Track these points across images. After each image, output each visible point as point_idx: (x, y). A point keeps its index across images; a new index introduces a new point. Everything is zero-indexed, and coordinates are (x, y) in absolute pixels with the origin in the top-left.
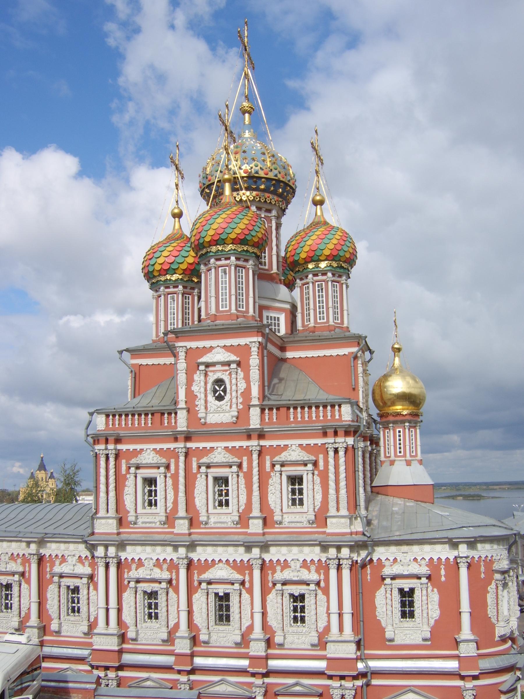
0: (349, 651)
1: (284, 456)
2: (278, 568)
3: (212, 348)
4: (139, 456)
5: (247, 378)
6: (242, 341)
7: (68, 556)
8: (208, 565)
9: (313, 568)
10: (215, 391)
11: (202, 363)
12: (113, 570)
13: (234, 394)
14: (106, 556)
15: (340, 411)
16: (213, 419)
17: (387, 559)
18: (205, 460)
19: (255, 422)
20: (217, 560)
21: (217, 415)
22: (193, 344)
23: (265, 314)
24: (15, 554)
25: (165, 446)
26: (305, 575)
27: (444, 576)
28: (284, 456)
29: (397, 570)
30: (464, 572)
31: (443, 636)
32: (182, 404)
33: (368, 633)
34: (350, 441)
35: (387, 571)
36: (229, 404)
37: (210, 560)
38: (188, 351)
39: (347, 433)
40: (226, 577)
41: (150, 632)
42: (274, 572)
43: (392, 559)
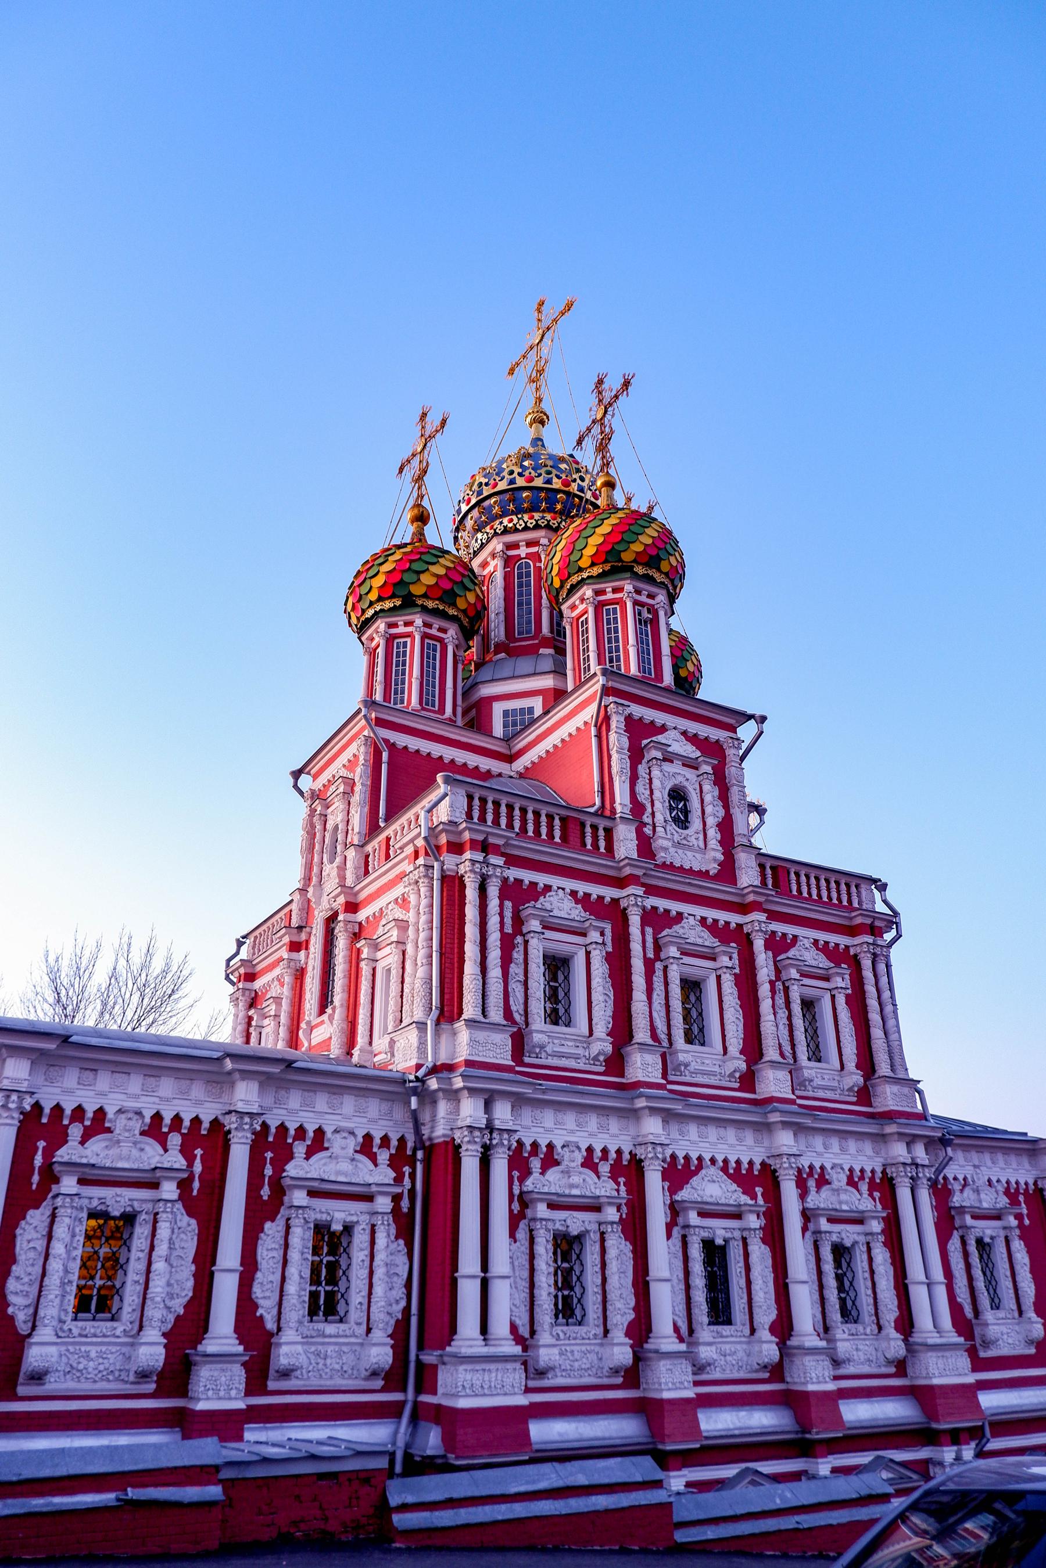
3: (663, 729)
4: (542, 898)
7: (336, 1131)
9: (864, 1187)
12: (500, 1167)
13: (711, 821)
14: (490, 1127)
15: (859, 896)
17: (955, 1179)
20: (707, 1157)
21: (680, 851)
22: (638, 711)
24: (168, 1118)
25: (596, 890)
27: (1028, 1215)
36: (701, 836)
37: (694, 1156)
40: (723, 1201)
41: (575, 1348)
43: (961, 1177)
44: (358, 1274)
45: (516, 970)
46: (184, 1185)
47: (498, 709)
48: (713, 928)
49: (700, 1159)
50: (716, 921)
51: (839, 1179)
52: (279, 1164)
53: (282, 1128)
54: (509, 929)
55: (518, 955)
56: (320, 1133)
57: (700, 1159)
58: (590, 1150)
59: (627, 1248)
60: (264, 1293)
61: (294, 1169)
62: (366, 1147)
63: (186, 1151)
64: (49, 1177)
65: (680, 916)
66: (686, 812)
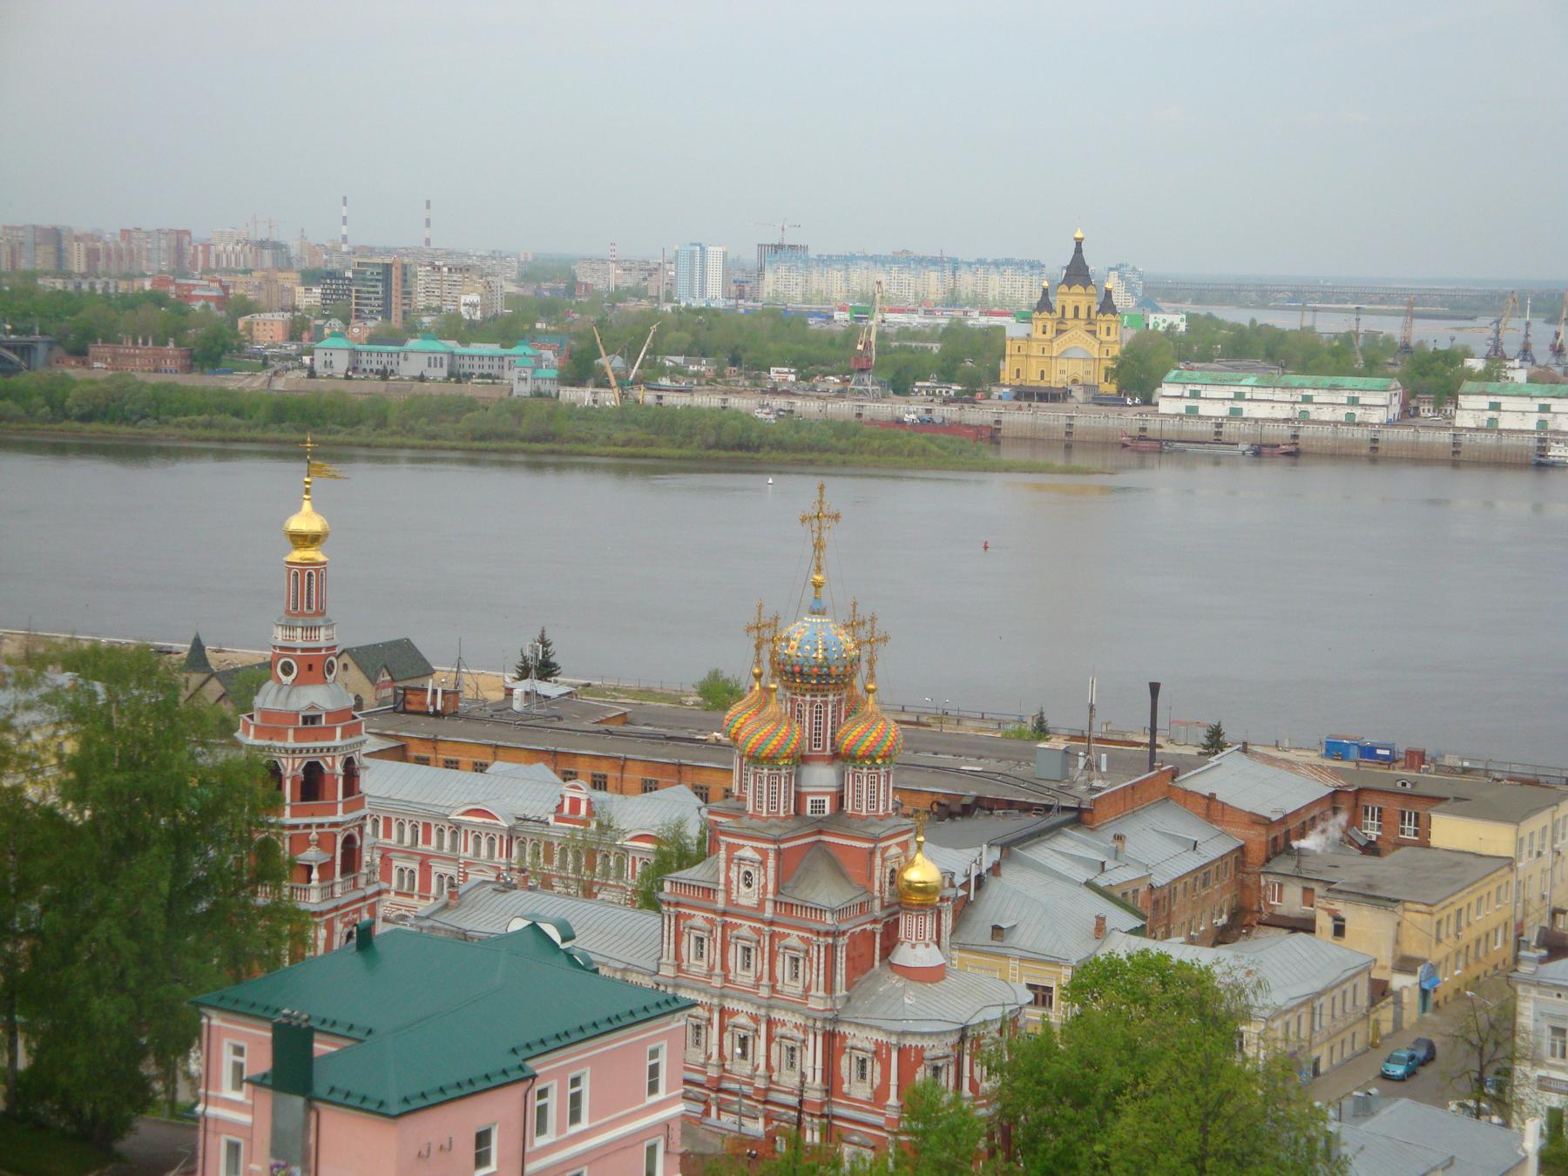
1: (787, 942)
6: (765, 846)
8: (734, 1013)
16: (743, 901)
22: (732, 840)
23: (809, 799)
28: (787, 942)
29: (855, 1042)
30: (894, 1055)
31: (880, 1096)
32: (722, 887)
34: (830, 940)
35: (849, 1042)
38: (728, 845)
39: (827, 934)
51: (790, 1025)
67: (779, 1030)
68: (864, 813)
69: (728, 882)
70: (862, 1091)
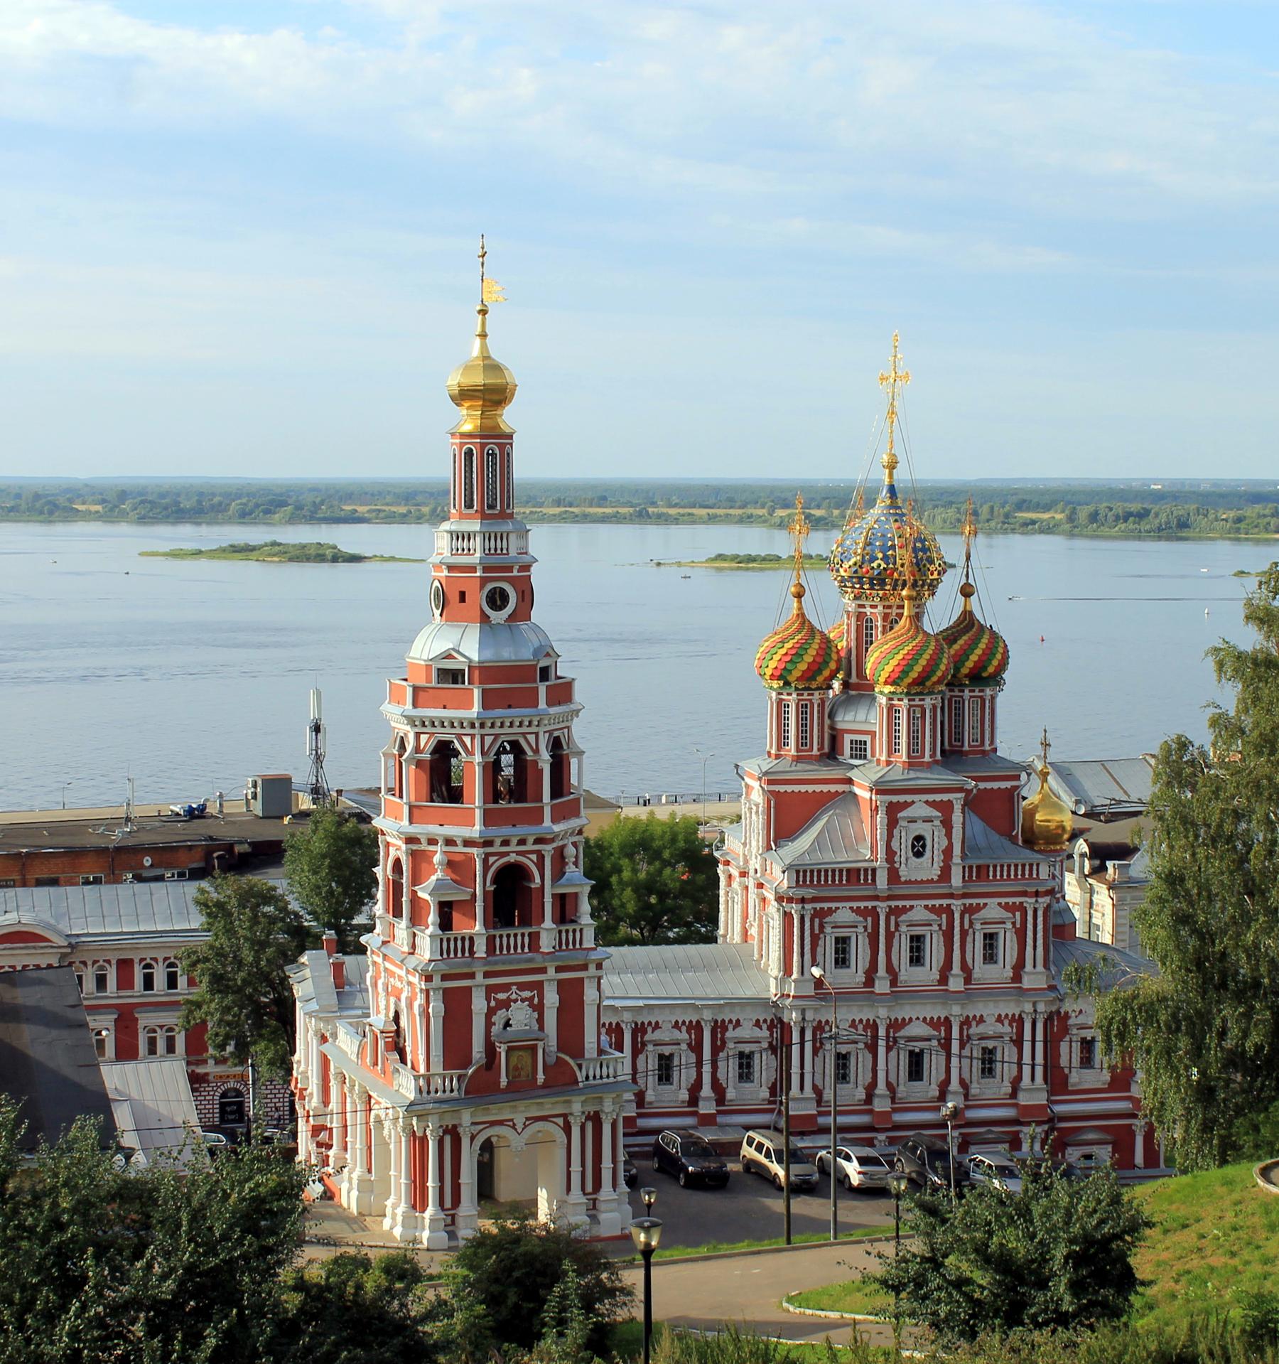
0: (1041, 1099)
2: (974, 1023)
3: (913, 802)
5: (949, 835)
6: (945, 797)
10: (913, 846)
11: (904, 818)
18: (903, 918)
19: (956, 880)
22: (895, 799)
25: (862, 905)
26: (1000, 1028)
29: (1081, 1020)
33: (1056, 1081)
42: (970, 1026)
44: (757, 1068)
45: (820, 950)
46: (689, 1045)
47: (848, 738)
48: (932, 909)
49: (911, 1019)
50: (934, 906)
51: (990, 1020)
52: (723, 1034)
53: (723, 1021)
54: (817, 931)
55: (821, 942)
56: (738, 1021)
57: (911, 1019)
58: (854, 1021)
59: (869, 1057)
60: (721, 1075)
61: (728, 1035)
62: (757, 1024)
63: (688, 1032)
64: (644, 1044)
65: (912, 907)
66: (924, 846)
67: (974, 1030)
68: (966, 748)
69: (890, 854)
70: (1098, 1077)
